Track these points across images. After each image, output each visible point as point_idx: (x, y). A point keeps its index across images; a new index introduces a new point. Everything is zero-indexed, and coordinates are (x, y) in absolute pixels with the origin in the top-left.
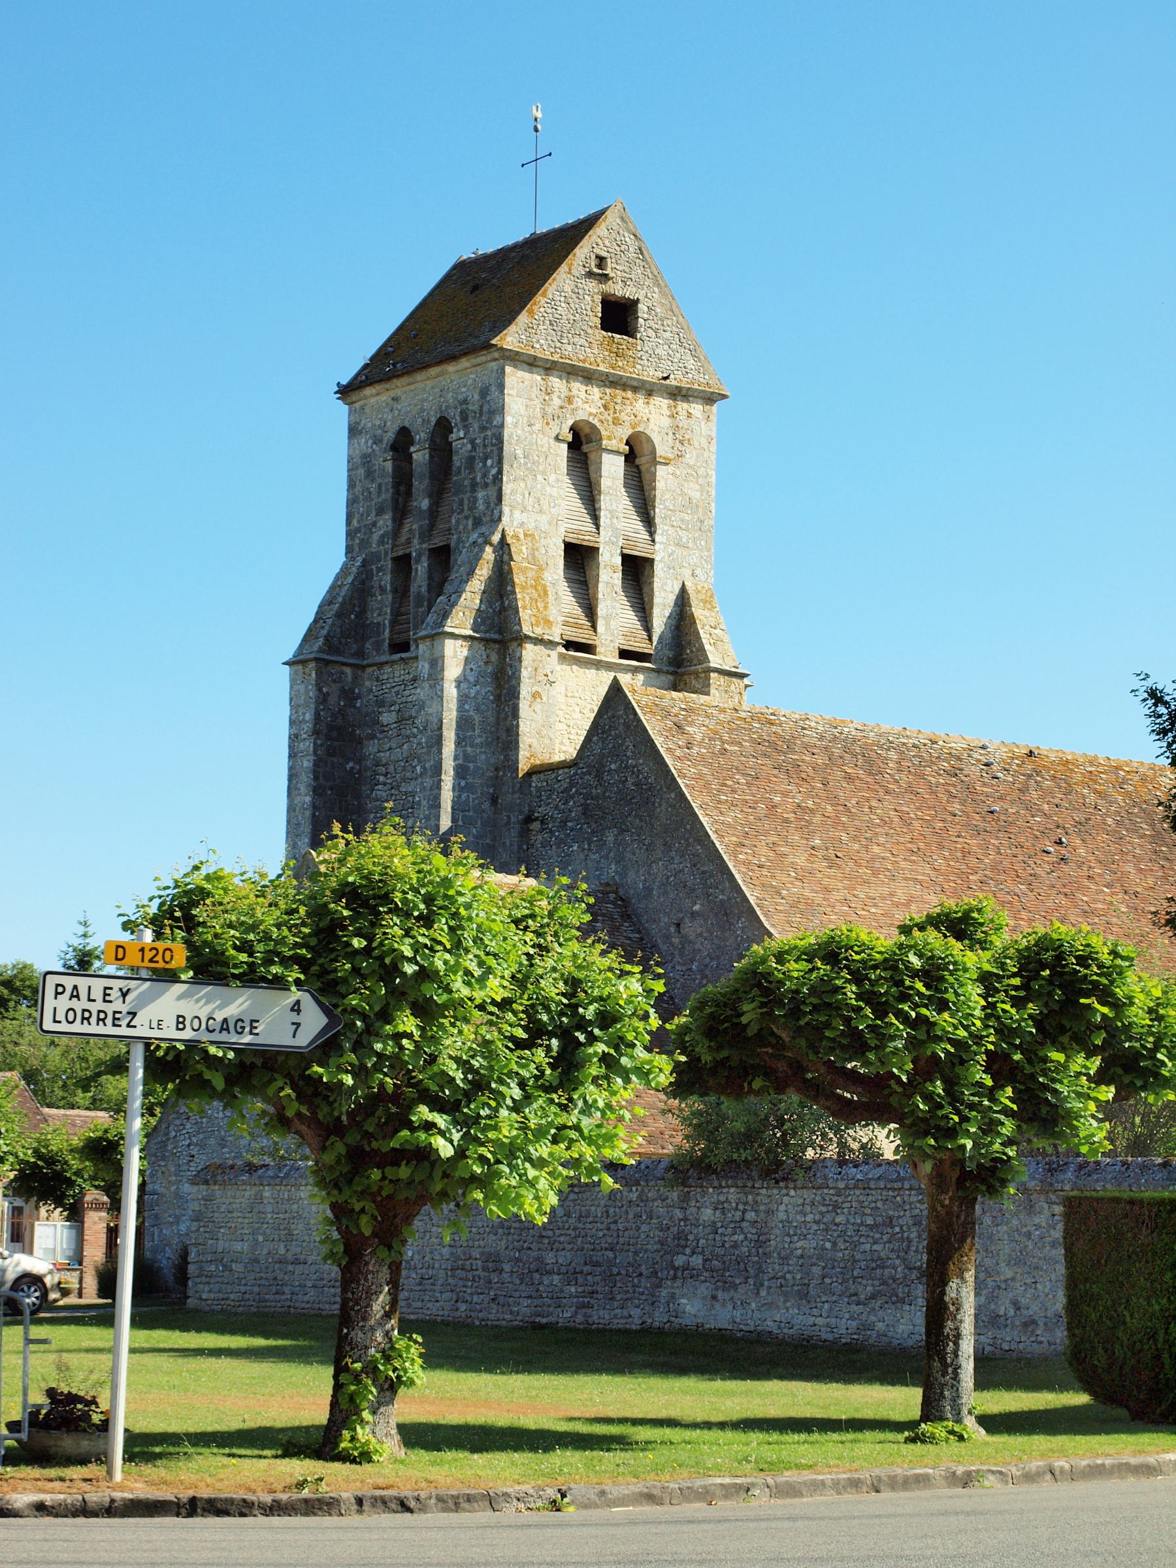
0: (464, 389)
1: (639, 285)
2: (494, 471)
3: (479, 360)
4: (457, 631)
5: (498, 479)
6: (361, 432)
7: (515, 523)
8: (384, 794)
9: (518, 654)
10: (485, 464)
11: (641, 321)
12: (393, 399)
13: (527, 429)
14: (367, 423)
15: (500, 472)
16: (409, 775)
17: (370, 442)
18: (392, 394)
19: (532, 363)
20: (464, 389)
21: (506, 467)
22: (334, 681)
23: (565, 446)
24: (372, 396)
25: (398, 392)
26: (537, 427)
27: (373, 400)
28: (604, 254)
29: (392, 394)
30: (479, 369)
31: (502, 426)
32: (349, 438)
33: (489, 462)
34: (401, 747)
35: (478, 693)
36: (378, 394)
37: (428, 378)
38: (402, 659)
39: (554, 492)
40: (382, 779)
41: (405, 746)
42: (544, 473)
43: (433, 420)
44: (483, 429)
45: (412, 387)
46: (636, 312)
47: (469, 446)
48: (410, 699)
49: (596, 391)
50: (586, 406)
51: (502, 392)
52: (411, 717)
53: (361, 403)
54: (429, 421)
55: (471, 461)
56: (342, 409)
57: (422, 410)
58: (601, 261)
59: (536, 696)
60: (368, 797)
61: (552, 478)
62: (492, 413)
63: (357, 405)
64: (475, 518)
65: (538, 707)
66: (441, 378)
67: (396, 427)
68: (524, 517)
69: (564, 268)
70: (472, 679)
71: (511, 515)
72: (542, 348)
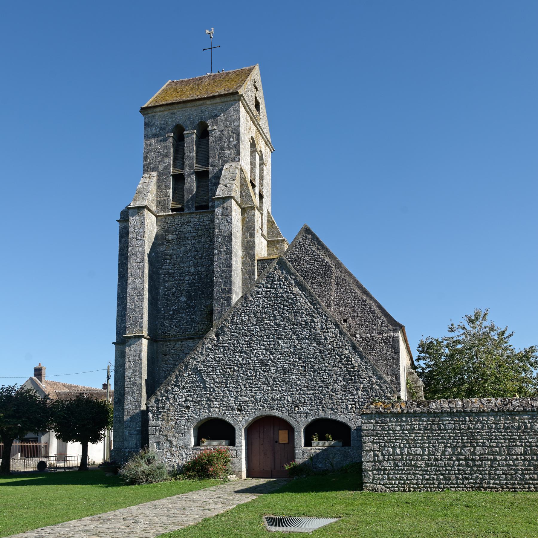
0: (215, 111)
2: (235, 142)
3: (226, 100)
6: (152, 125)
9: (252, 213)
12: (172, 114)
17: (158, 130)
20: (215, 111)
24: (160, 111)
27: (159, 114)
29: (171, 111)
30: (224, 104)
31: (239, 125)
32: (145, 128)
33: (231, 139)
36: (163, 111)
37: (195, 106)
38: (181, 214)
40: (168, 261)
43: (197, 122)
45: (183, 109)
47: (219, 133)
53: (153, 114)
54: (194, 123)
55: (220, 138)
57: (189, 118)
66: (201, 107)
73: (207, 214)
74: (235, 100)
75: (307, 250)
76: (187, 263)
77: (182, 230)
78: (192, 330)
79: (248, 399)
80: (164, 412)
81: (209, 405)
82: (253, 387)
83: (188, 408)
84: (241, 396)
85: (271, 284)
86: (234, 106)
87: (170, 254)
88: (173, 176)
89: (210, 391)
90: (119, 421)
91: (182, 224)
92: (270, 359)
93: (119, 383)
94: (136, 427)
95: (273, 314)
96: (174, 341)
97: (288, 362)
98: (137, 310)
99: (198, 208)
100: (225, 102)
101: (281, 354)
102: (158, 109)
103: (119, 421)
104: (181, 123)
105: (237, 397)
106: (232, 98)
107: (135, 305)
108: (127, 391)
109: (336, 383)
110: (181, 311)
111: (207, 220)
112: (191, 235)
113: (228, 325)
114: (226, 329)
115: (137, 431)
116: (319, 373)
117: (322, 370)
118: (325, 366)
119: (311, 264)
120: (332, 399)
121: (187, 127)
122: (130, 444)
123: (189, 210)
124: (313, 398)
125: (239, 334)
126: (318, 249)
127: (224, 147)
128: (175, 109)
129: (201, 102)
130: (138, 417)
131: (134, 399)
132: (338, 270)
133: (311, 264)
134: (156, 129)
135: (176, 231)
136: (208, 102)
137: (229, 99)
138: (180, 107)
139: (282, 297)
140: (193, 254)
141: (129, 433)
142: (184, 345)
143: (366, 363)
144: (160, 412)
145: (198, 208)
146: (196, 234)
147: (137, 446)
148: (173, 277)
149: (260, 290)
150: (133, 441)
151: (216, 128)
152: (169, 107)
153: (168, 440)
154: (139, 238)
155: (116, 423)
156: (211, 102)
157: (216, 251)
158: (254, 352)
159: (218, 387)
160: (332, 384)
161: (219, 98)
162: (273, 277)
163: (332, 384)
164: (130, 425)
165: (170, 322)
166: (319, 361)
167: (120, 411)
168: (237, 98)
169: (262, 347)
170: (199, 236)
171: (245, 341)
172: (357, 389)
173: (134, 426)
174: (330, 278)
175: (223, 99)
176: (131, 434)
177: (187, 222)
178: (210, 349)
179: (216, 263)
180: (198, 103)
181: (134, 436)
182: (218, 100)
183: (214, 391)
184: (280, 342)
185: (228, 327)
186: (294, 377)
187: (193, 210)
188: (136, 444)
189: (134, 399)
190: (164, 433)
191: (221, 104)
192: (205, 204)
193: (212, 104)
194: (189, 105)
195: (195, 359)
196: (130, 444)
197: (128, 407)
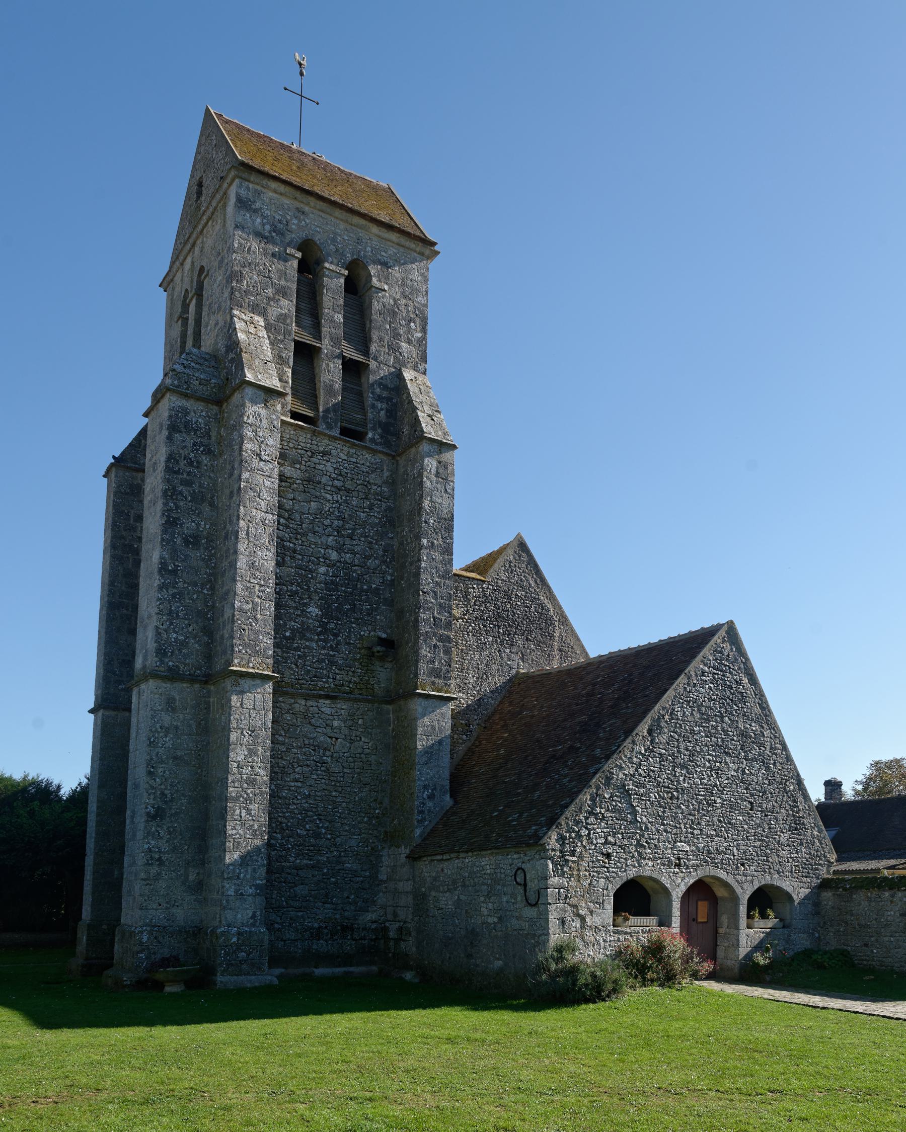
0: (383, 254)
2: (419, 335)
30: (402, 250)
37: (347, 222)
45: (323, 215)
47: (392, 302)
73: (364, 452)
74: (422, 254)
75: (521, 580)
76: (324, 539)
77: (313, 465)
78: (330, 680)
79: (688, 848)
80: (573, 862)
81: (640, 854)
82: (694, 829)
83: (608, 856)
84: (681, 841)
85: (718, 663)
86: (417, 264)
89: (641, 829)
90: (159, 859)
91: (312, 453)
92: (716, 785)
93: (160, 770)
94: (254, 878)
95: (720, 712)
96: (293, 696)
97: (736, 794)
98: (259, 616)
99: (345, 432)
100: (403, 246)
101: (728, 779)
102: (274, 185)
103: (159, 859)
105: (675, 842)
106: (419, 247)
107: (255, 605)
108: (233, 795)
109: (783, 833)
110: (308, 635)
111: (363, 464)
112: (330, 483)
113: (667, 717)
114: (663, 724)
115: (257, 887)
116: (766, 815)
117: (769, 812)
118: (774, 806)
119: (527, 607)
120: (778, 856)
121: (329, 255)
122: (239, 916)
123: (328, 428)
124: (759, 853)
125: (680, 736)
126: (536, 582)
128: (308, 204)
129: (362, 222)
130: (258, 856)
131: (250, 815)
132: (562, 627)
133: (527, 607)
136: (375, 229)
137: (413, 246)
138: (318, 207)
140: (336, 523)
141: (236, 891)
142: (311, 709)
143: (809, 807)
144: (567, 861)
145: (345, 432)
146: (342, 484)
147: (256, 921)
148: (292, 558)
149: (706, 669)
150: (247, 909)
151: (386, 287)
152: (298, 194)
153: (578, 915)
154: (267, 458)
155: (152, 864)
156: (381, 234)
157: (425, 541)
158: (698, 770)
159: (650, 822)
160: (779, 833)
161: (398, 235)
162: (721, 652)
163: (779, 833)
164: (239, 874)
165: (283, 652)
166: (767, 798)
167: (162, 838)
168: (427, 252)
169: (707, 764)
170: (348, 490)
171: (687, 750)
172: (801, 844)
173: (248, 876)
174: (552, 637)
175: (403, 240)
176: (242, 894)
177: (325, 453)
178: (643, 755)
179: (423, 565)
180: (356, 220)
181: (250, 898)
182: (394, 236)
183: (647, 828)
184: (728, 759)
185: (666, 722)
186: (741, 818)
187: (336, 433)
188: (254, 916)
189: (250, 815)
190: (573, 901)
191: (397, 247)
192: (361, 429)
193: (379, 237)
194: (338, 213)
195: (621, 768)
196: (239, 916)
197: (234, 832)
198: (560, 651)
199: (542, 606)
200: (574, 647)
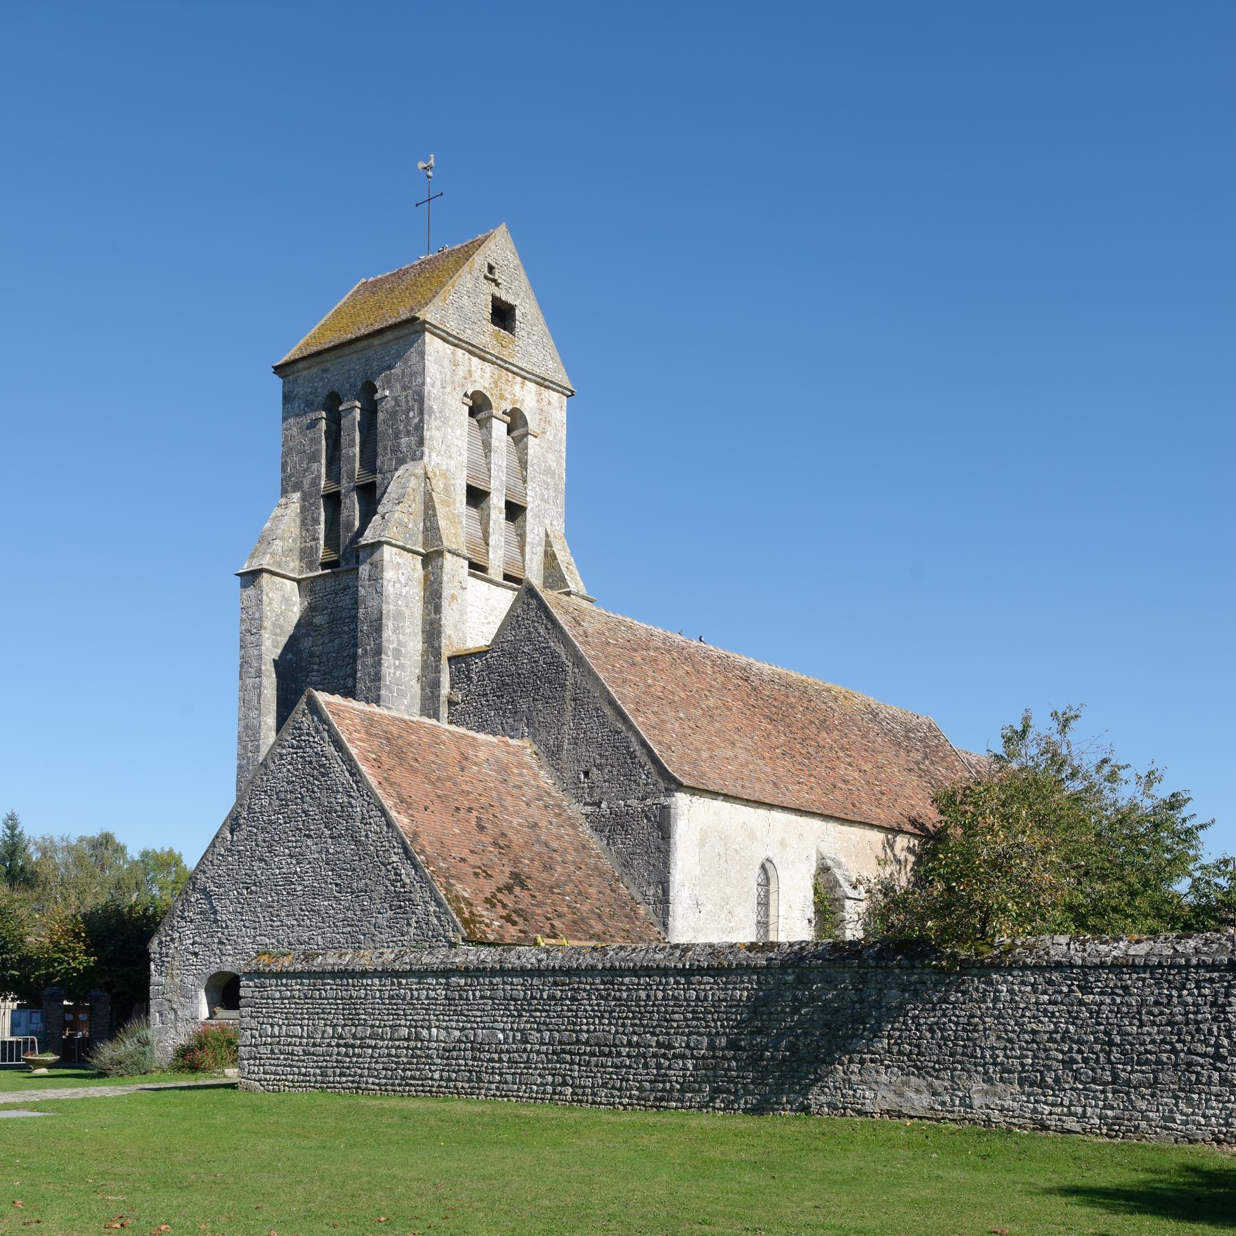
0: (387, 358)
1: (517, 295)
2: (416, 420)
4: (393, 542)
5: (419, 428)
6: (294, 398)
7: (433, 463)
8: (318, 679)
9: (440, 564)
10: (407, 416)
11: (517, 322)
13: (441, 390)
14: (300, 391)
15: (422, 421)
16: (340, 663)
17: (303, 405)
18: (322, 366)
19: (446, 337)
20: (387, 358)
21: (426, 416)
22: (277, 589)
23: (467, 408)
24: (305, 369)
25: (328, 365)
26: (448, 390)
27: (304, 373)
28: (494, 265)
29: (322, 366)
31: (423, 384)
33: (411, 414)
34: (332, 641)
35: (407, 592)
36: (309, 368)
37: (355, 352)
39: (459, 443)
40: (315, 667)
41: (336, 641)
42: (452, 427)
44: (404, 388)
45: (339, 360)
46: (514, 315)
47: (393, 403)
48: (341, 604)
49: (488, 367)
50: (482, 381)
51: (423, 358)
52: (341, 618)
53: (295, 375)
54: (356, 385)
55: (393, 415)
56: (279, 381)
57: (349, 377)
58: (491, 268)
59: (453, 597)
60: (304, 681)
61: (458, 432)
62: (414, 375)
63: (291, 378)
64: (397, 459)
65: (455, 607)
67: (326, 392)
68: (439, 460)
69: (466, 268)
70: (403, 582)
71: (430, 456)
72: (452, 326)
74: (417, 332)
75: (530, 633)
79: (268, 941)
80: (168, 962)
81: (221, 950)
82: (274, 921)
83: (196, 954)
84: (260, 935)
85: (298, 741)
86: (416, 345)
87: (318, 653)
88: (323, 496)
89: (222, 928)
92: (296, 873)
95: (300, 793)
97: (319, 877)
98: (251, 768)
101: (310, 863)
102: (301, 365)
104: (336, 389)
105: (255, 937)
107: (248, 758)
109: (380, 913)
113: (245, 814)
114: (242, 821)
116: (357, 896)
117: (362, 891)
118: (366, 884)
119: (535, 662)
120: (374, 941)
121: (345, 395)
124: (349, 939)
125: (258, 829)
126: (546, 628)
127: (400, 432)
128: (327, 361)
129: (364, 343)
132: (577, 671)
133: (535, 662)
134: (299, 406)
135: (327, 608)
136: (376, 341)
137: (406, 331)
139: (311, 762)
143: (421, 877)
144: (163, 961)
149: (284, 751)
151: (387, 393)
152: (317, 359)
153: (173, 1009)
156: (381, 341)
157: (360, 651)
158: (276, 859)
159: (230, 920)
160: (374, 915)
162: (300, 729)
163: (374, 915)
166: (358, 876)
168: (418, 328)
169: (287, 851)
171: (265, 842)
172: (409, 925)
174: (563, 686)
175: (397, 333)
177: (344, 589)
178: (222, 856)
179: (359, 675)
182: (389, 336)
183: (227, 927)
184: (309, 842)
185: (244, 818)
186: (326, 903)
190: (169, 996)
193: (382, 344)
194: (346, 350)
195: (205, 872)
198: (574, 700)
199: (554, 654)
200: (592, 690)
